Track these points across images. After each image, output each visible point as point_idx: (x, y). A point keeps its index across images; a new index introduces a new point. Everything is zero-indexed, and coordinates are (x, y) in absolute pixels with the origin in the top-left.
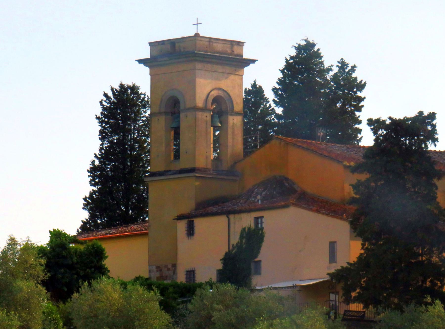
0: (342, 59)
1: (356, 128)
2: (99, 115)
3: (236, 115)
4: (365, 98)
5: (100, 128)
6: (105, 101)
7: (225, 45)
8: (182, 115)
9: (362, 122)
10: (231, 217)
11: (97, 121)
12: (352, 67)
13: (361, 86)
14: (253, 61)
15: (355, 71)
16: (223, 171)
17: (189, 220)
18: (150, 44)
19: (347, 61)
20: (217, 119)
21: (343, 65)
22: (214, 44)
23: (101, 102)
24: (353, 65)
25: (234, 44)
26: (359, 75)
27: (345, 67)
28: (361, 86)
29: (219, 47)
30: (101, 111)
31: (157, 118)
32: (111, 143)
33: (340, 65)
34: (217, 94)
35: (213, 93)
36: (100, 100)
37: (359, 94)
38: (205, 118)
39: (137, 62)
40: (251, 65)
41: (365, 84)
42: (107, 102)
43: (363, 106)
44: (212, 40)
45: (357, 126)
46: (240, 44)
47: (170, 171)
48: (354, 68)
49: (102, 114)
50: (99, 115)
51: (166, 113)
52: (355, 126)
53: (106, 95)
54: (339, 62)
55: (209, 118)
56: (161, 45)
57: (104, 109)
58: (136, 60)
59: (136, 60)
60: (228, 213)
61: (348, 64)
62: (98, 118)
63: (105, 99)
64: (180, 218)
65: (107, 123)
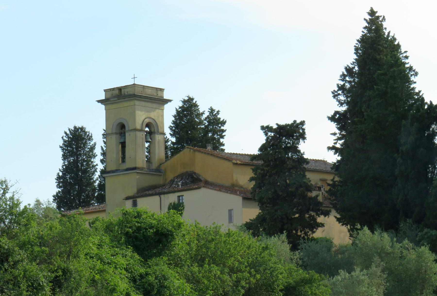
0: (211, 107)
1: (221, 148)
2: (61, 145)
3: (161, 135)
4: (226, 130)
5: (62, 153)
6: (65, 137)
7: (153, 91)
8: (127, 134)
9: (225, 145)
10: (162, 196)
11: (60, 149)
12: (217, 111)
13: (224, 123)
14: (170, 101)
15: (220, 114)
16: (153, 169)
17: (134, 199)
18: (105, 91)
19: (214, 108)
20: (148, 137)
21: (212, 110)
22: (146, 90)
23: (62, 138)
24: (218, 110)
25: (158, 90)
26: (221, 116)
27: (213, 112)
28: (224, 123)
29: (149, 92)
30: (62, 143)
31: (110, 137)
32: (69, 162)
33: (210, 111)
34: (149, 121)
35: (146, 120)
36: (62, 136)
37: (222, 128)
38: (142, 136)
39: (97, 102)
40: (169, 103)
41: (226, 122)
42: (66, 137)
43: (225, 135)
44: (145, 87)
45: (222, 147)
46: (162, 90)
47: (119, 170)
48: (218, 112)
49: (63, 144)
50: (61, 145)
51: (116, 133)
52: (221, 148)
53: (66, 133)
54: (209, 109)
55: (144, 136)
56: (112, 91)
57: (65, 141)
58: (96, 101)
59: (96, 101)
60: (160, 194)
61: (215, 110)
62: (61, 147)
63: (65, 135)
64: (128, 198)
65: (66, 150)
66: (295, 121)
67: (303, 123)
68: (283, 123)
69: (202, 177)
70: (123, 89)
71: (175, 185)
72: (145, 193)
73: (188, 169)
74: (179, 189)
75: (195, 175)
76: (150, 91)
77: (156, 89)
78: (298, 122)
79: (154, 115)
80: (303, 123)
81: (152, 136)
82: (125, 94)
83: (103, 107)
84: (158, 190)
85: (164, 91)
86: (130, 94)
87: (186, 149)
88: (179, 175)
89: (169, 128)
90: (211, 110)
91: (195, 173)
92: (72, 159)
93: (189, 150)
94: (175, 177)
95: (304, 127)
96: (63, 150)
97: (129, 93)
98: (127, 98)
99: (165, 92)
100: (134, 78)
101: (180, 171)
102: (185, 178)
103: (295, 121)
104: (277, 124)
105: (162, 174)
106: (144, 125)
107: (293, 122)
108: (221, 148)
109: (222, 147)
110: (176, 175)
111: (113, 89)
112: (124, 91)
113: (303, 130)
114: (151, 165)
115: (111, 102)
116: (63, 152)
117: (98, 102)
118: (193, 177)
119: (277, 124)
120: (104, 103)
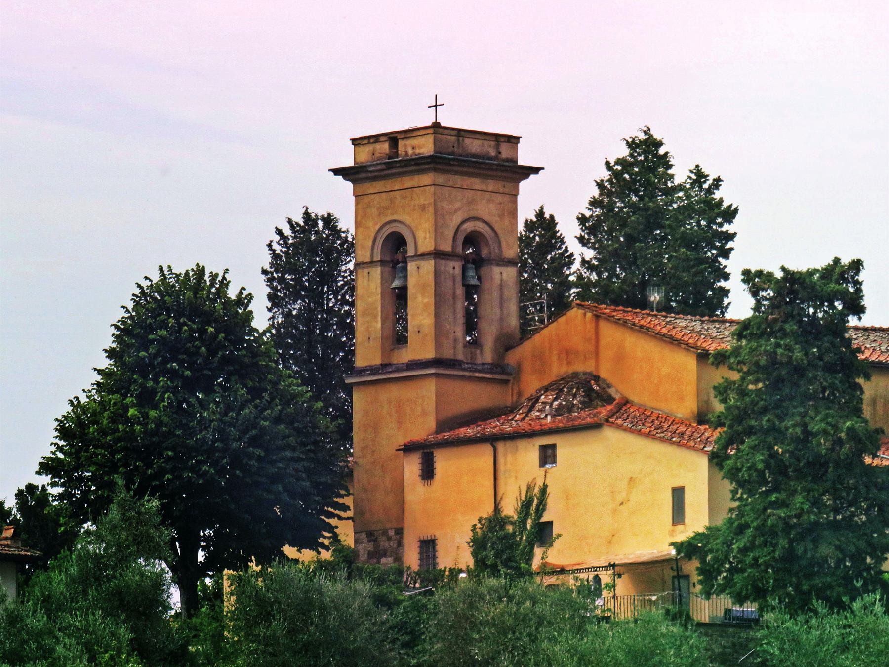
0: (697, 166)
1: (720, 287)
2: (267, 267)
3: (507, 266)
4: (735, 234)
5: (268, 290)
6: (278, 243)
7: (486, 143)
8: (411, 266)
9: (731, 277)
11: (264, 277)
12: (714, 180)
13: (730, 214)
14: (536, 170)
15: (720, 188)
16: (483, 364)
17: (425, 451)
18: (355, 142)
19: (705, 170)
20: (471, 273)
21: (699, 176)
22: (468, 141)
23: (270, 245)
24: (716, 177)
25: (502, 140)
26: (726, 195)
27: (703, 180)
28: (730, 214)
29: (474, 146)
30: (269, 259)
31: (366, 271)
32: (288, 315)
33: (694, 177)
34: (473, 229)
35: (465, 226)
36: (268, 242)
37: (726, 227)
38: (451, 271)
39: (332, 174)
40: (533, 177)
41: (736, 210)
42: (280, 244)
43: (732, 249)
44: (463, 133)
45: (722, 283)
46: (513, 141)
47: (390, 365)
48: (717, 182)
49: (272, 265)
50: (267, 267)
51: (382, 263)
52: (719, 284)
53: (279, 232)
54: (691, 172)
55: (458, 271)
56: (373, 143)
57: (275, 256)
58: (330, 170)
59: (330, 170)
60: (493, 440)
61: (708, 176)
62: (264, 272)
63: (277, 238)
64: (408, 448)
65: (281, 280)
66: (837, 261)
67: (857, 265)
68: (799, 265)
69: (617, 391)
70: (402, 139)
71: (539, 411)
72: (457, 431)
73: (582, 367)
74: (543, 427)
75: (598, 385)
76: (479, 142)
77: (494, 139)
78: (845, 261)
79: (486, 209)
80: (857, 265)
81: (484, 271)
82: (406, 152)
83: (349, 185)
84: (493, 426)
85: (518, 142)
86: (419, 154)
87: (575, 309)
88: (551, 384)
89: (578, 219)
90: (696, 174)
91: (599, 377)
92: (296, 307)
93: (581, 312)
94: (540, 390)
95: (861, 277)
96: (270, 280)
97: (417, 151)
98: (413, 165)
99: (521, 146)
100: (436, 106)
101: (558, 369)
102: (568, 392)
103: (837, 261)
104: (783, 269)
105: (510, 378)
106: (460, 242)
107: (831, 263)
108: (719, 284)
109: (722, 283)
110: (546, 383)
111: (375, 139)
112: (405, 146)
113: (858, 284)
114: (478, 352)
115: (370, 175)
116: (271, 288)
117: (335, 175)
118: (589, 391)
119: (783, 269)
120: (352, 177)
